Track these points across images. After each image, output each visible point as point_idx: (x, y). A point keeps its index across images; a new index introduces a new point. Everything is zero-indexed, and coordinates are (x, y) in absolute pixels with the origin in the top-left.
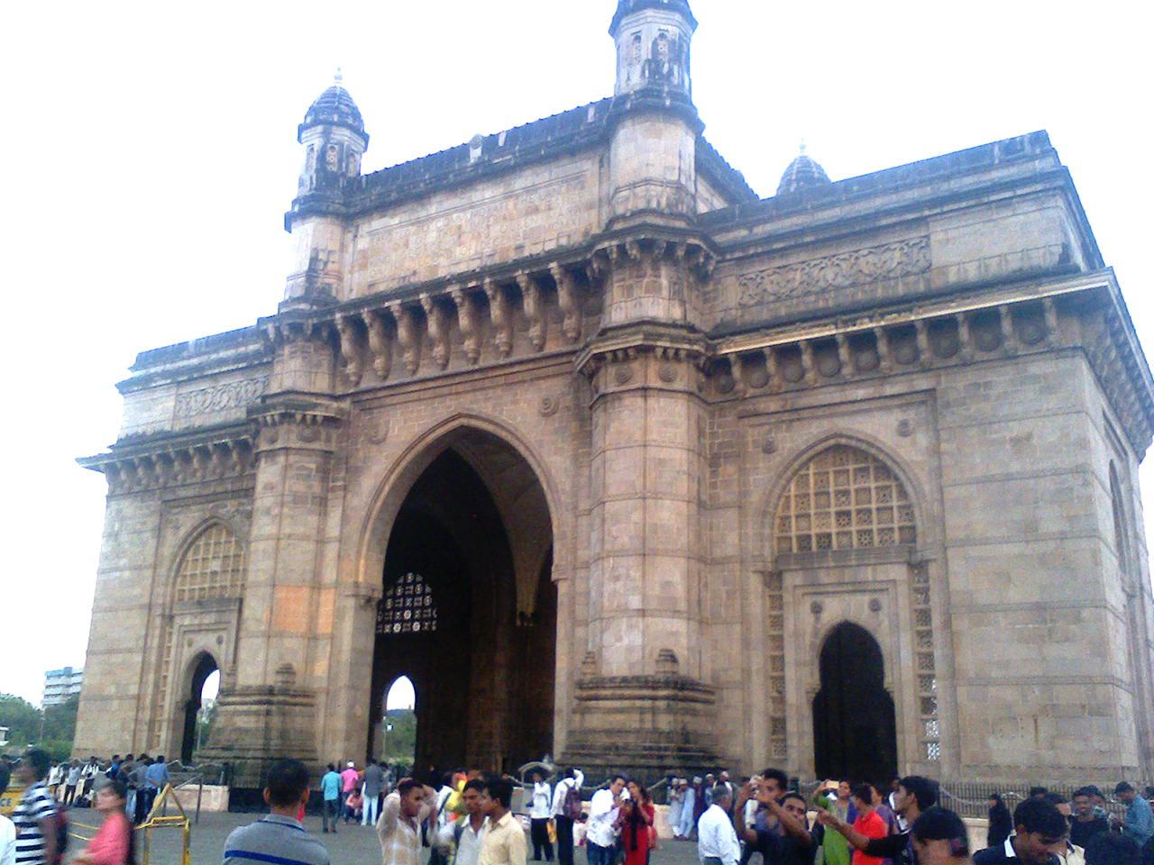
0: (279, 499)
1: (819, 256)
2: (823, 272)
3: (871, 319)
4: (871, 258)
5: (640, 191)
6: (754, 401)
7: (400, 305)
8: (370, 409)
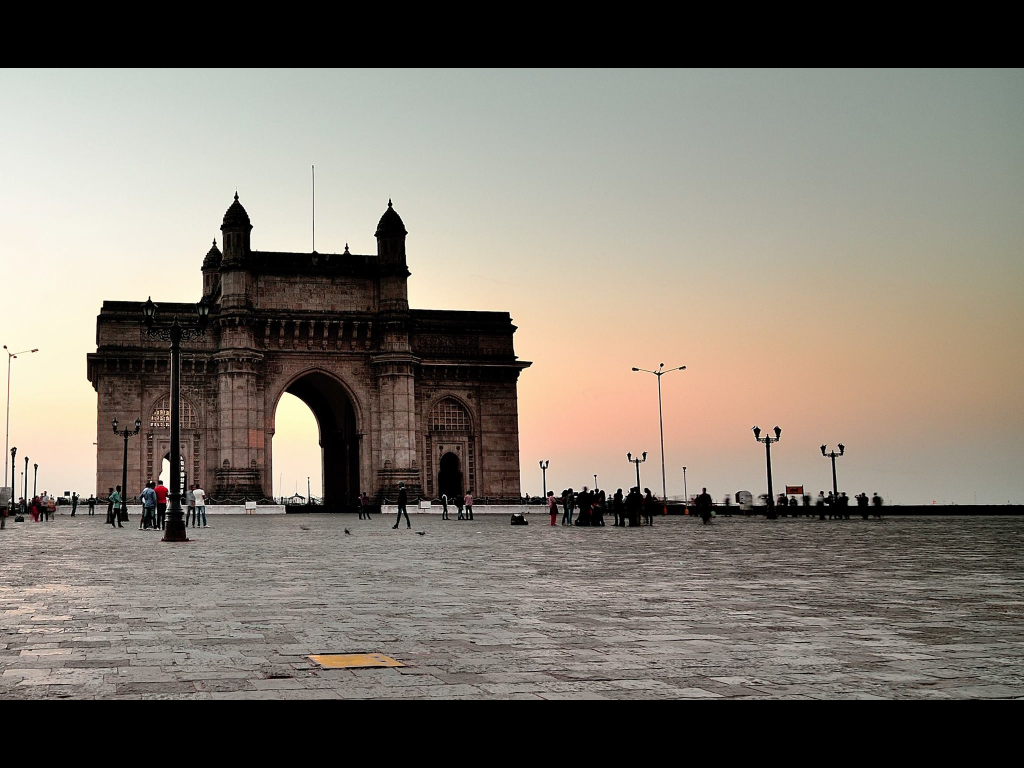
5: (400, 302)
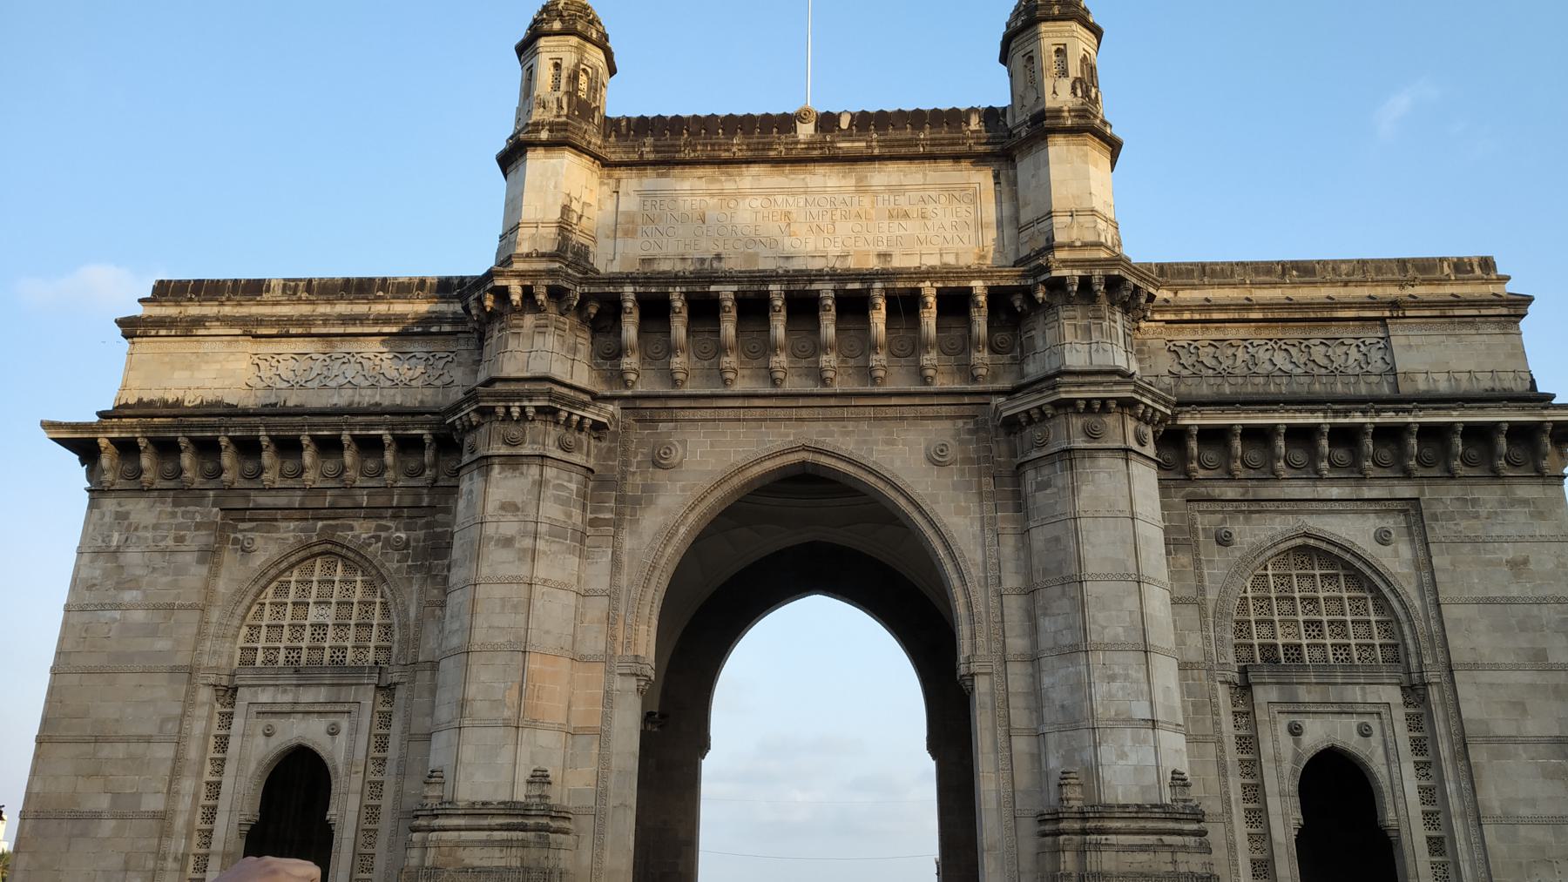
0: (531, 527)
1: (1263, 336)
2: (1268, 355)
3: (1364, 413)
4: (1322, 349)
6: (1209, 483)
7: (735, 292)
8: (652, 421)
